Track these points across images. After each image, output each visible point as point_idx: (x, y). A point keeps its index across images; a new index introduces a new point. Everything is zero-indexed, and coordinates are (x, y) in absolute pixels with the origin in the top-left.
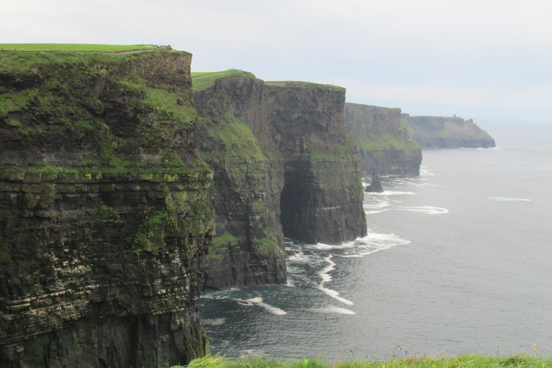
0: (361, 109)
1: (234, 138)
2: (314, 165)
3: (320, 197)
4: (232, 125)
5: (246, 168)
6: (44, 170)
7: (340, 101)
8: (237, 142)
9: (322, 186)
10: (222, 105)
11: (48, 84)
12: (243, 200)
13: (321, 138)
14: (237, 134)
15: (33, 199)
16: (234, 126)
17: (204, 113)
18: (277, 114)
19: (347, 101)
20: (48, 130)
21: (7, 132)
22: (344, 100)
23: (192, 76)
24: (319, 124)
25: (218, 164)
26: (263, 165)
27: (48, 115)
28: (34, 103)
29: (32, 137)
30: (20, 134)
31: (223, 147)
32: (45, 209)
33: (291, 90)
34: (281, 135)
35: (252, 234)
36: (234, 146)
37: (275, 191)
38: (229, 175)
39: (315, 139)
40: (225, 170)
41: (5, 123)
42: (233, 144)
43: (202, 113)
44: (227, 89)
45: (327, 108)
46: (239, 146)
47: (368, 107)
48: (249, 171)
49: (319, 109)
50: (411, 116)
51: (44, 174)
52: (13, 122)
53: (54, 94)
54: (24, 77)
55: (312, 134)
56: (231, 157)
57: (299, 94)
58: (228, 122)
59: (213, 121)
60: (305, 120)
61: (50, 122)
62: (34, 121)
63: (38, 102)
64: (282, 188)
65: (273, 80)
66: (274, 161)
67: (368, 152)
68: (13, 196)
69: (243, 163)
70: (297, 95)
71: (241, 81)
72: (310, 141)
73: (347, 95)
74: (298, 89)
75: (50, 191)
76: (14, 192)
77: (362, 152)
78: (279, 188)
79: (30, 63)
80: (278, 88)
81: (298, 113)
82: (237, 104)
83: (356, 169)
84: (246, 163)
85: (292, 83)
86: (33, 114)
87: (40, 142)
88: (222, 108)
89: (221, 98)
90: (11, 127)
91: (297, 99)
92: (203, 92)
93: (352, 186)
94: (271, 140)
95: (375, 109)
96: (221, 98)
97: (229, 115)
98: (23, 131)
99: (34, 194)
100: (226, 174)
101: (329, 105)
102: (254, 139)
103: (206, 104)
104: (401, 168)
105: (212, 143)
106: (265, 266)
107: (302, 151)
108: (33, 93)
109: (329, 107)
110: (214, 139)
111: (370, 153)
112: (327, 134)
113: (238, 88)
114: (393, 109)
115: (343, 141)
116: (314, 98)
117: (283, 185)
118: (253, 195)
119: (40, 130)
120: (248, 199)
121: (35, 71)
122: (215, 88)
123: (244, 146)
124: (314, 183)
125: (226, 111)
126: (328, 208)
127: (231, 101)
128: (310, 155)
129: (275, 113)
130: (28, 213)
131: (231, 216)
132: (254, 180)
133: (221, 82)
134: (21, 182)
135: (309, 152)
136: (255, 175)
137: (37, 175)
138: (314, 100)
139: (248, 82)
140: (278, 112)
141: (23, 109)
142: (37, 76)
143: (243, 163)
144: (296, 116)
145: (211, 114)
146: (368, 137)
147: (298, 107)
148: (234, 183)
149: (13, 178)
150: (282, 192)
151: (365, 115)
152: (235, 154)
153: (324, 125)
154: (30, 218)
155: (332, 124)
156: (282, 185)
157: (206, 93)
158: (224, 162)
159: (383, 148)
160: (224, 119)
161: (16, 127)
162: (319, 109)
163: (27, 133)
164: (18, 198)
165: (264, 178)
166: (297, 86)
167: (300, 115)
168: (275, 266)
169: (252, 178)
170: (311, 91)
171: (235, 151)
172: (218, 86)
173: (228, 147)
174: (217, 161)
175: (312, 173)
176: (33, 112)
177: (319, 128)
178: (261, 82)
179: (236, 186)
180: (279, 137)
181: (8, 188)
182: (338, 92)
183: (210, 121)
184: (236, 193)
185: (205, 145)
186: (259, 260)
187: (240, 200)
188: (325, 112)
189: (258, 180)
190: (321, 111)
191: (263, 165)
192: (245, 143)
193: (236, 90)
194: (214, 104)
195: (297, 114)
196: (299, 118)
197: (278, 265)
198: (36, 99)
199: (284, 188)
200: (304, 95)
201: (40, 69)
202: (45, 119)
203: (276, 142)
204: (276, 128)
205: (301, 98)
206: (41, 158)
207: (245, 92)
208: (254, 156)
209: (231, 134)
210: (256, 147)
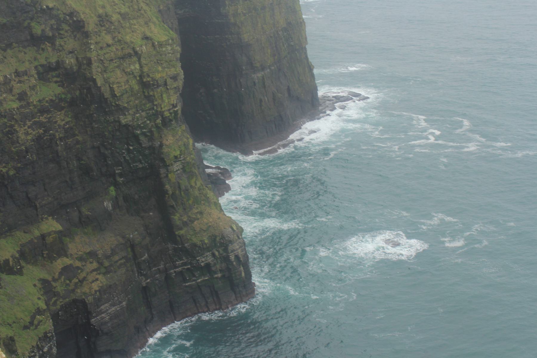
5: (137, 66)
8: (109, 9)
12: (142, 138)
25: (75, 68)
26: (169, 48)
31: (78, 27)
35: (173, 207)
36: (103, 20)
40: (94, 81)
42: (100, 16)
46: (115, 17)
48: (146, 69)
56: (101, 48)
84: (136, 53)
105: (53, 22)
106: (208, 266)
118: (159, 121)
120: (151, 132)
123: (124, 16)
126: (260, 75)
131: (121, 175)
136: (158, 76)
143: (130, 56)
148: (118, 105)
152: (108, 39)
158: (89, 62)
168: (226, 259)
171: (108, 32)
173: (91, 27)
179: (122, 110)
184: (127, 126)
185: (37, 29)
186: (195, 258)
187: (136, 137)
189: (166, 84)
191: (169, 48)
197: (232, 258)
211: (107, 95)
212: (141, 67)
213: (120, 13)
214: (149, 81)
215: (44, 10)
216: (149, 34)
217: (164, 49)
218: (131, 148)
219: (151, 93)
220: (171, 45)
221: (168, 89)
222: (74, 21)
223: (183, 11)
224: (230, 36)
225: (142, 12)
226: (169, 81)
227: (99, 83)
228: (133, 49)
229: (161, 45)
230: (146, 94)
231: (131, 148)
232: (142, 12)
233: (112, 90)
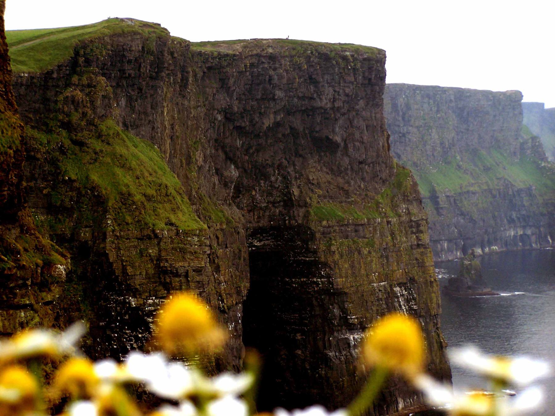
0: (428, 96)
1: (126, 179)
2: (318, 235)
3: (336, 311)
4: (120, 150)
7: (373, 80)
8: (133, 189)
9: (340, 282)
10: (92, 102)
13: (332, 170)
14: (130, 169)
16: (124, 151)
17: (52, 124)
18: (226, 118)
19: (389, 80)
22: (383, 78)
23: (8, 41)
24: (327, 138)
26: (196, 239)
31: (99, 201)
33: (254, 60)
34: (237, 167)
36: (125, 198)
37: (228, 302)
38: (117, 268)
39: (316, 172)
43: (46, 124)
44: (105, 65)
45: (343, 98)
46: (138, 197)
47: (444, 90)
48: (163, 254)
49: (324, 102)
50: (547, 107)
55: (311, 161)
57: (275, 69)
58: (108, 144)
59: (75, 142)
60: (291, 128)
64: (245, 292)
65: (212, 39)
66: (222, 230)
67: (447, 197)
69: (149, 238)
70: (271, 72)
71: (136, 46)
72: (309, 180)
73: (389, 66)
74: (272, 58)
77: (434, 198)
78: (239, 293)
80: (221, 56)
81: (275, 113)
82: (130, 100)
83: (418, 239)
84: (156, 236)
85: (257, 43)
88: (94, 109)
89: (89, 86)
91: (270, 79)
92: (48, 75)
93: (412, 280)
94: (216, 179)
95: (460, 94)
96: (89, 86)
97: (111, 125)
100: (111, 264)
101: (347, 90)
102: (171, 181)
103: (56, 102)
104: (529, 232)
107: (288, 202)
109: (347, 95)
110: (76, 185)
111: (455, 201)
112: (347, 160)
113: (129, 62)
114: (504, 94)
115: (384, 175)
116: (310, 78)
117: (248, 285)
122: (74, 64)
123: (149, 198)
124: (322, 277)
125: (103, 117)
127: (115, 94)
128: (308, 212)
129: (219, 118)
132: (177, 275)
133: (88, 50)
135: (306, 205)
138: (312, 80)
139: (153, 46)
140: (229, 116)
143: (149, 238)
144: (268, 122)
145: (68, 126)
146: (449, 163)
147: (274, 99)
150: (244, 303)
151: (438, 111)
153: (338, 139)
155: (357, 135)
156: (245, 285)
157: (55, 75)
159: (485, 187)
160: (99, 136)
162: (325, 101)
165: (199, 271)
166: (270, 50)
167: (279, 118)
169: (172, 272)
170: (302, 60)
172: (81, 60)
174: (85, 234)
175: (315, 252)
177: (325, 146)
178: (185, 45)
180: (233, 172)
182: (368, 60)
183: (67, 143)
188: (339, 109)
189: (187, 276)
190: (329, 105)
192: (150, 192)
193: (127, 67)
194: (73, 102)
195: (272, 116)
196: (277, 125)
199: (250, 291)
200: (287, 71)
203: (226, 185)
204: (226, 153)
205: (280, 77)
207: (146, 69)
208: (173, 219)
209: (119, 171)
210: (179, 199)
211: (118, 272)
212: (160, 251)
213: (145, 195)
214: (166, 267)
215: (66, 181)
216: (174, 221)
217: (189, 239)
218: (140, 336)
219: (168, 280)
220: (198, 236)
221: (188, 281)
222: (94, 196)
223: (262, 243)
224: (319, 280)
225: (171, 198)
226: (191, 273)
227: (112, 257)
228: (153, 231)
229: (186, 233)
230: (163, 280)
231: (140, 336)
232: (171, 198)
233: (124, 269)
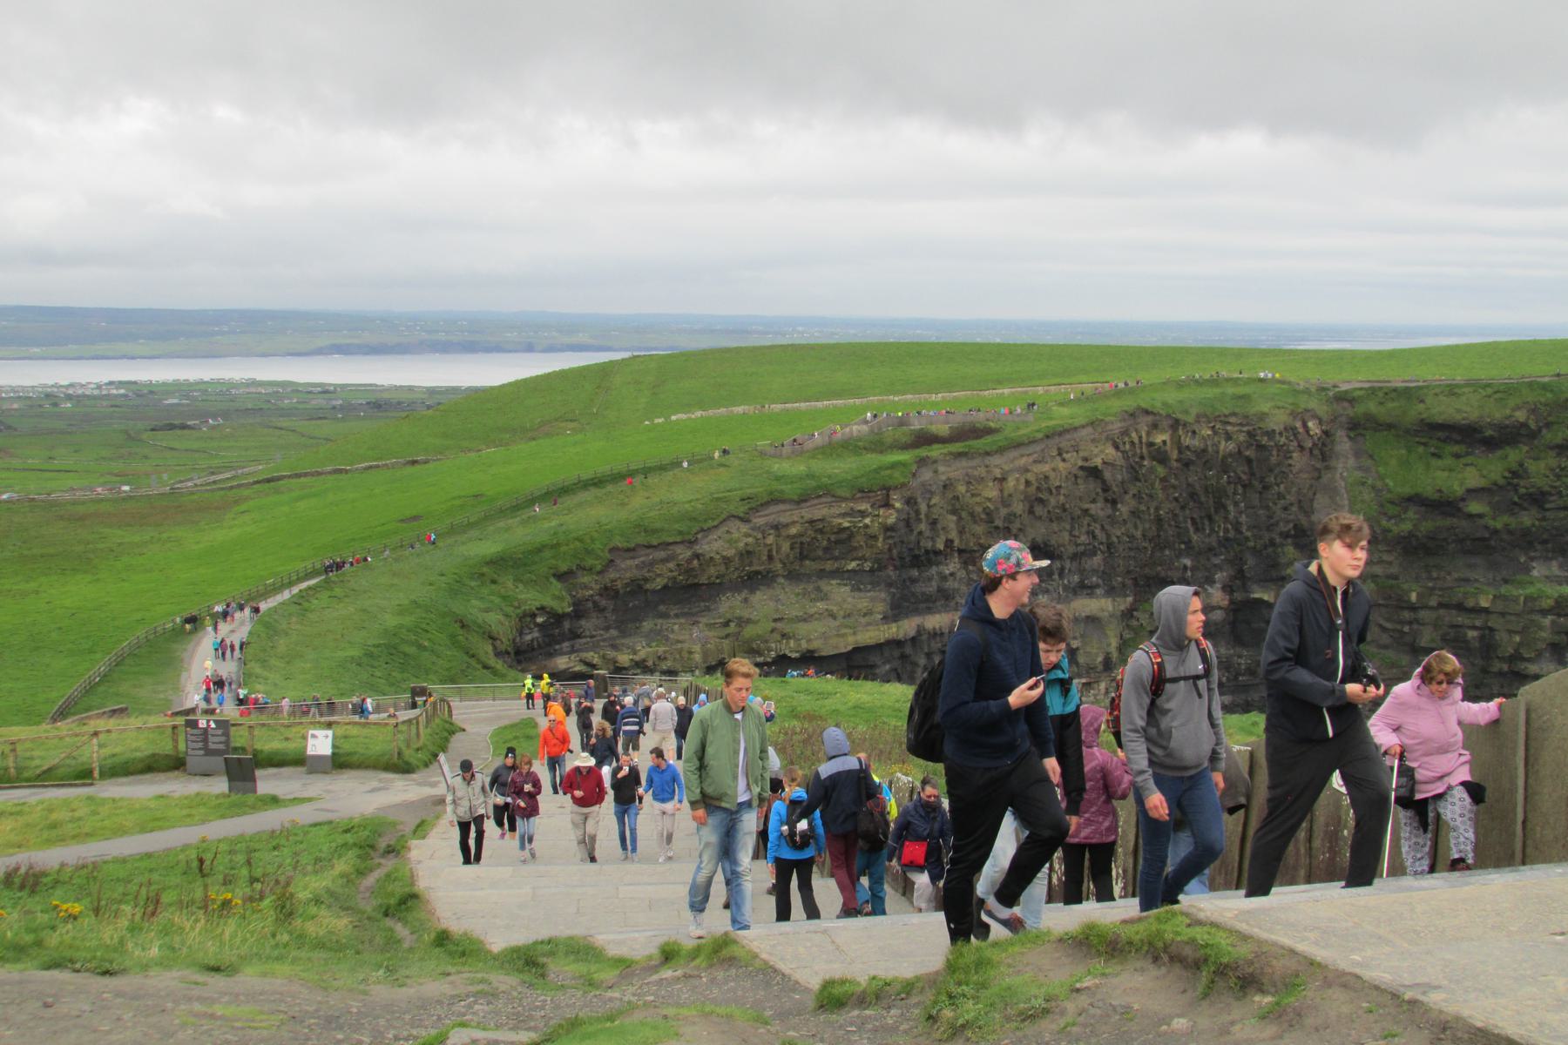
6: (1530, 590)
11: (1548, 436)
15: (1508, 642)
20: (1544, 519)
21: (1464, 523)
27: (1543, 494)
28: (1517, 473)
29: (1510, 532)
30: (1486, 527)
32: (1529, 660)
41: (1459, 510)
51: (1528, 599)
52: (1474, 507)
53: (1559, 455)
54: (1501, 427)
61: (1548, 506)
62: (1515, 503)
63: (1526, 471)
68: (1472, 634)
75: (1541, 628)
76: (1474, 628)
79: (1512, 402)
86: (1511, 493)
87: (1526, 541)
90: (1470, 516)
98: (1491, 523)
99: (1510, 632)
108: (1514, 455)
119: (1527, 519)
121: (1521, 416)
130: (1498, 666)
134: (1486, 611)
137: (1515, 600)
141: (1495, 484)
142: (1524, 425)
149: (1470, 603)
154: (1501, 674)
161: (1480, 516)
163: (1499, 525)
164: (1482, 638)
176: (1516, 487)
181: (1460, 619)
198: (1521, 465)
201: (1533, 411)
202: (1538, 499)
206: (1527, 570)
